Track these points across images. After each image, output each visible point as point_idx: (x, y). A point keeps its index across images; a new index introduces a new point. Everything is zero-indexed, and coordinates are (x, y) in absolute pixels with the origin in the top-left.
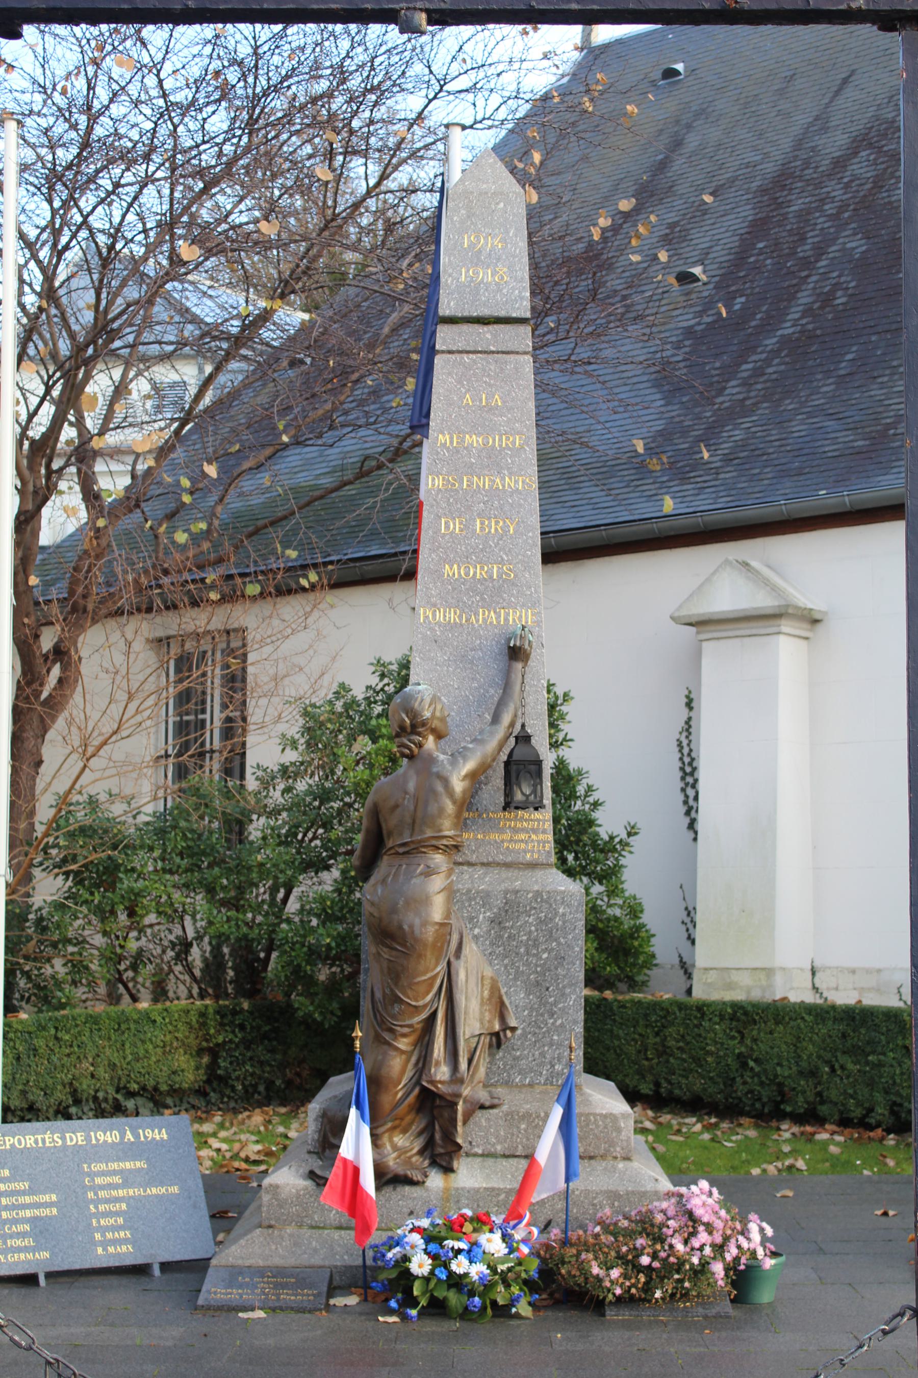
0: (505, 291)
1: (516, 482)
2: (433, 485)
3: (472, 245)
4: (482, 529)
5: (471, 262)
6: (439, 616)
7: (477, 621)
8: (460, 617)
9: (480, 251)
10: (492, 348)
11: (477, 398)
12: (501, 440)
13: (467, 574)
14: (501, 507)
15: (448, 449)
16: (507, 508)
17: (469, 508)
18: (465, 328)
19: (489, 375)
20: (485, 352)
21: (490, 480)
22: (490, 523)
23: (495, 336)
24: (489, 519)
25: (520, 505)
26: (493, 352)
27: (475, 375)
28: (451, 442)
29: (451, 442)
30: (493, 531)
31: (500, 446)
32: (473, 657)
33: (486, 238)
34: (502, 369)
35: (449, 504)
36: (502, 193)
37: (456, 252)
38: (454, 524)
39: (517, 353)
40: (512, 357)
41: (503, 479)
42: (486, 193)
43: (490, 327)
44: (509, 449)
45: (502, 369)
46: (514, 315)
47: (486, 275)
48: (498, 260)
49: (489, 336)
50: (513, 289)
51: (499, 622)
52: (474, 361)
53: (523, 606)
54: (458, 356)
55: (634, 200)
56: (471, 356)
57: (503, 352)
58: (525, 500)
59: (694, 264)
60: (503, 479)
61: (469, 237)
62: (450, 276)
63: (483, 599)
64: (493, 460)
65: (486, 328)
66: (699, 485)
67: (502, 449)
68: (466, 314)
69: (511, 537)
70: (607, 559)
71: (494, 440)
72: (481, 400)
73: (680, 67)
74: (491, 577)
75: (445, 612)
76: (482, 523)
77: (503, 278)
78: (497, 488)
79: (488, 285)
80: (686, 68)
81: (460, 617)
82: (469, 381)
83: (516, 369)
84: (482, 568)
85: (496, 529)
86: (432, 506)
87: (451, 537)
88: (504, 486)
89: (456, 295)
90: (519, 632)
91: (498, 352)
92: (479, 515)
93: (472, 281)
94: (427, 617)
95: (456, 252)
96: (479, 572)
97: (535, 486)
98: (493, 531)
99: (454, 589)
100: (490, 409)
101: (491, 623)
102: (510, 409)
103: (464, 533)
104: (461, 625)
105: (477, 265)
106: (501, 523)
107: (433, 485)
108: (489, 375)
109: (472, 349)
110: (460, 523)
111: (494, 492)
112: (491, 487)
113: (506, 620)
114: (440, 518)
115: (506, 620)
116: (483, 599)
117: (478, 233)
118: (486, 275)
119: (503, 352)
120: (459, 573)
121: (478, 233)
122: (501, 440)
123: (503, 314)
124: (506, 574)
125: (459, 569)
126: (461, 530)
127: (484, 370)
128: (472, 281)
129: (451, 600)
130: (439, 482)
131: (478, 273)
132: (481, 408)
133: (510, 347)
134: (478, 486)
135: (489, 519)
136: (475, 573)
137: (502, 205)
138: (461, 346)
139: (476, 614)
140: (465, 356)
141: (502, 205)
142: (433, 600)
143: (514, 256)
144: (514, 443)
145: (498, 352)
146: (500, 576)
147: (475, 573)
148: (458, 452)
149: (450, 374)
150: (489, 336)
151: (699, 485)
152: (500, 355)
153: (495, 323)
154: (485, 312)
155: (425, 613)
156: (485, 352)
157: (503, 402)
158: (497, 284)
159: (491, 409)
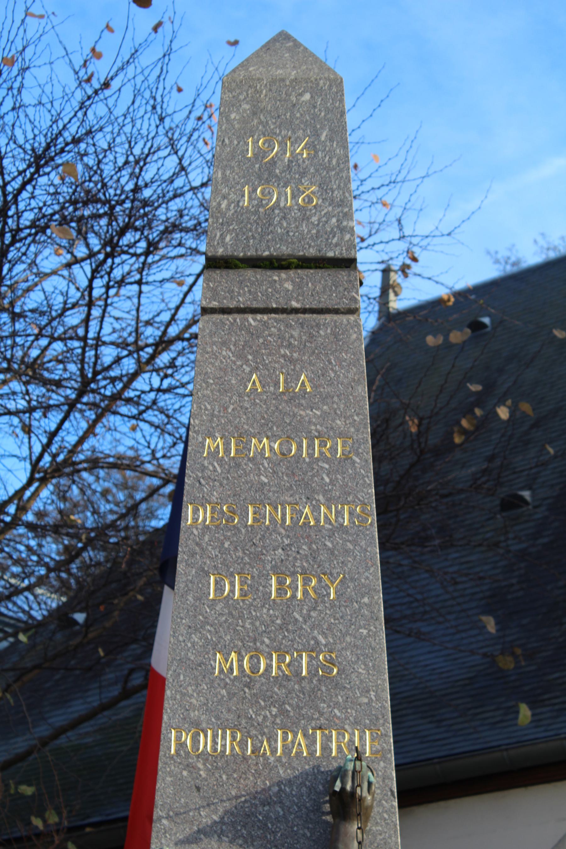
0: (314, 219)
1: (339, 514)
2: (195, 520)
3: (259, 154)
4: (281, 591)
5: (260, 178)
6: (205, 743)
7: (274, 751)
8: (243, 744)
9: (273, 162)
10: (295, 304)
11: (269, 380)
12: (311, 446)
13: (255, 668)
14: (314, 555)
15: (221, 461)
16: (323, 556)
17: (257, 557)
18: (249, 273)
19: (290, 345)
20: (283, 311)
21: (293, 510)
22: (294, 581)
23: (299, 286)
24: (293, 574)
25: (347, 551)
26: (296, 311)
27: (266, 344)
28: (227, 450)
29: (227, 450)
30: (299, 595)
31: (311, 455)
32: (267, 817)
33: (282, 144)
34: (311, 336)
35: (223, 551)
36: (307, 80)
37: (233, 163)
38: (232, 584)
39: (336, 311)
40: (328, 317)
41: (316, 509)
42: (283, 80)
43: (292, 273)
44: (327, 460)
45: (311, 336)
46: (330, 254)
47: (282, 197)
48: (303, 174)
49: (288, 286)
50: (329, 216)
51: (312, 753)
52: (265, 324)
53: (356, 723)
54: (238, 317)
55: (468, 331)
56: (259, 317)
57: (313, 311)
58: (355, 543)
59: (522, 489)
60: (316, 509)
61: (256, 142)
62: (224, 197)
63: (283, 712)
64: (299, 479)
65: (283, 275)
66: (557, 707)
67: (313, 461)
68: (251, 253)
69: (332, 606)
70: (442, 804)
71: (300, 447)
72: (277, 384)
73: (486, 320)
74: (298, 673)
75: (215, 736)
76: (281, 583)
77: (310, 201)
78: (306, 524)
79: (285, 212)
80: (492, 321)
81: (243, 744)
82: (256, 354)
83: (335, 335)
84: (281, 659)
85: (305, 592)
86: (193, 554)
87: (227, 605)
88: (317, 520)
89: (234, 226)
90: (350, 766)
91: (304, 311)
92: (276, 570)
93: (260, 204)
94: (181, 745)
95: (233, 163)
96: (272, 665)
97: (372, 519)
98: (299, 595)
99: (231, 695)
100: (292, 399)
101: (299, 753)
102: (325, 398)
103: (249, 599)
104: (245, 758)
105: (268, 181)
106: (314, 582)
107: (195, 520)
108: (290, 345)
109: (261, 305)
110: (242, 583)
111: (300, 531)
112: (295, 522)
113: (326, 748)
114: (207, 574)
115: (326, 748)
116: (283, 712)
117: (270, 136)
118: (282, 197)
119: (313, 311)
120: (241, 666)
121: (270, 136)
122: (311, 446)
123: (312, 252)
124: (323, 667)
125: (240, 660)
126: (244, 594)
127: (281, 337)
128: (260, 204)
129: (225, 715)
130: (205, 515)
131: (270, 194)
132: (277, 396)
133: (325, 301)
134: (272, 520)
135: (293, 574)
136: (269, 667)
137: (307, 96)
138: (242, 301)
139: (272, 739)
140: (250, 318)
141: (307, 96)
142: (194, 714)
143: (329, 169)
144: (334, 450)
145: (304, 311)
146: (312, 672)
147: (269, 667)
148: (238, 465)
149: (224, 343)
150: (288, 286)
151: (557, 707)
152: (307, 316)
153: (298, 267)
154: (284, 250)
155: (178, 738)
156: (283, 311)
157: (315, 387)
158: (301, 209)
159: (293, 398)
